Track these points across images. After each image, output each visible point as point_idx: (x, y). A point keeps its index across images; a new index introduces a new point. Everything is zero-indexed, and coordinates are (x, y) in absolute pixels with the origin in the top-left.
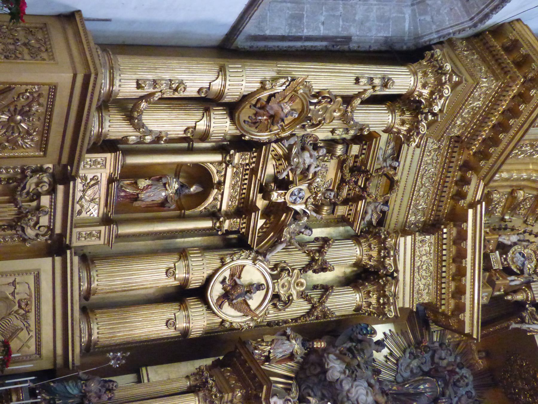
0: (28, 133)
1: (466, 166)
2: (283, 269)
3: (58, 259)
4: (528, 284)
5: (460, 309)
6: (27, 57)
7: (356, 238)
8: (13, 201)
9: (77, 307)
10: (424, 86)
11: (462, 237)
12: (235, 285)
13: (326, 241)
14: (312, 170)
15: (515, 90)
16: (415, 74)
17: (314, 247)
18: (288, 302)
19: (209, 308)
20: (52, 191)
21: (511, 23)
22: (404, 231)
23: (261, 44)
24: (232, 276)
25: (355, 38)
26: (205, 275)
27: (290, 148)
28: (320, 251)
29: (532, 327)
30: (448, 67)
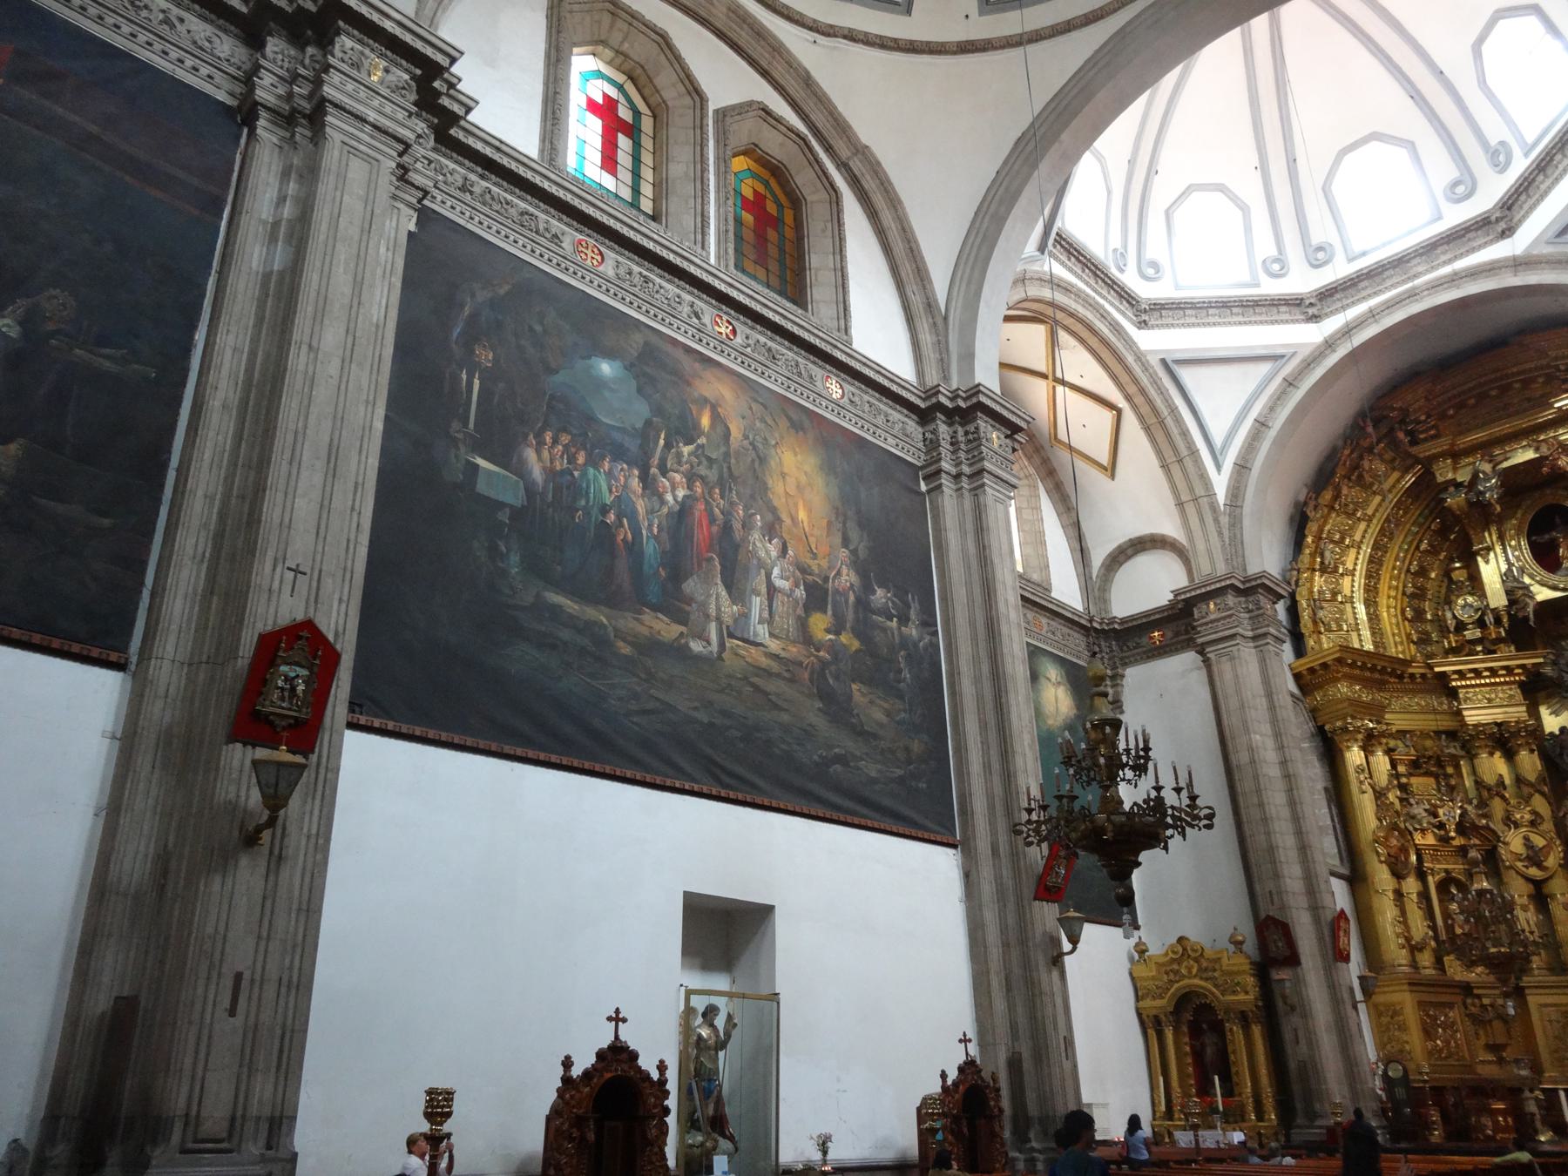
0: (1446, 1016)
1: (1401, 677)
2: (1508, 818)
3: (1527, 991)
4: (1493, 610)
5: (1522, 666)
6: (1401, 1018)
7: (1472, 757)
8: (1490, 1021)
9: (1562, 978)
10: (1356, 740)
11: (1461, 675)
12: (1528, 858)
13: (1479, 783)
14: (1428, 807)
15: (1346, 670)
16: (1348, 747)
17: (1485, 794)
18: (1534, 812)
19: (1551, 877)
20: (1479, 997)
21: (1291, 669)
22: (1459, 713)
23: (1344, 854)
24: (1520, 860)
25: (1324, 785)
26: (1521, 881)
27: (1416, 830)
28: (1489, 789)
29: (1530, 609)
30: (1339, 724)
